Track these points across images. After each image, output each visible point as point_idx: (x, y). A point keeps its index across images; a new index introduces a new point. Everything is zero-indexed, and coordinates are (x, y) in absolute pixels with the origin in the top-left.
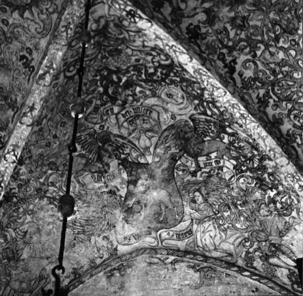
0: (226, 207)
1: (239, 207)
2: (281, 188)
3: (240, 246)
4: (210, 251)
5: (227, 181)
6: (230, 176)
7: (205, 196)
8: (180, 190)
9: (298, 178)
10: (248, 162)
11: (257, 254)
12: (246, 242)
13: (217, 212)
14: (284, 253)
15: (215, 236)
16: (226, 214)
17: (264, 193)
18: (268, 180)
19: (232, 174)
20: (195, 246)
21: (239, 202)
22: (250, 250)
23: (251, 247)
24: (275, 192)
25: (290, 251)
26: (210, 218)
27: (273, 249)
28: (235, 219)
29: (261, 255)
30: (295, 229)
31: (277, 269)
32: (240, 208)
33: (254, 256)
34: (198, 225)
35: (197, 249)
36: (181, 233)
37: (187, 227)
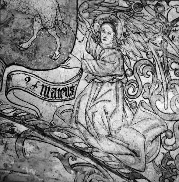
0: (149, 69)
1: (172, 73)
3: (154, 142)
4: (97, 137)
5: (169, 24)
7: (119, 37)
8: (81, 9)
12: (167, 137)
13: (129, 72)
15: (114, 112)
16: (144, 80)
20: (71, 120)
22: (171, 152)
26: (113, 79)
28: (156, 92)
32: (173, 76)
34: (89, 83)
35: (74, 126)
36: (51, 87)
37: (68, 79)
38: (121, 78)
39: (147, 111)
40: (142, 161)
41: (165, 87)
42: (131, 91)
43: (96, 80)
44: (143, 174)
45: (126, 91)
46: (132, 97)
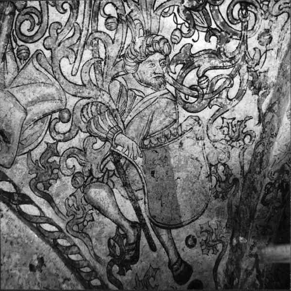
1: (102, 20)
3: (40, 123)
11: (71, 162)
12: (60, 119)
14: (126, 185)
17: (185, 30)
22: (60, 144)
23: (65, 140)
24: (213, 44)
25: (141, 186)
27: (111, 166)
28: (67, 43)
29: (79, 168)
30: (181, 144)
31: (95, 217)
32: (102, 27)
33: (63, 165)
39: (43, 70)
40: (11, 151)
41: (83, 39)
42: (25, 27)
44: (8, 172)
45: (18, 24)
46: (25, 38)
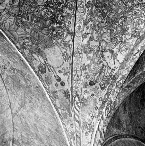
0: (27, 17)
1: (34, 21)
2: (62, 25)
3: (22, 38)
6: (41, 4)
9: (81, 22)
10: (56, 4)
12: (26, 38)
13: (20, 16)
15: (12, 25)
16: (24, 20)
18: (59, 18)
19: (43, 4)
21: (35, 19)
23: (27, 43)
24: (58, 25)
29: (30, 49)
38: (17, 16)
41: (30, 25)
42: (19, 21)
43: (9, 13)
